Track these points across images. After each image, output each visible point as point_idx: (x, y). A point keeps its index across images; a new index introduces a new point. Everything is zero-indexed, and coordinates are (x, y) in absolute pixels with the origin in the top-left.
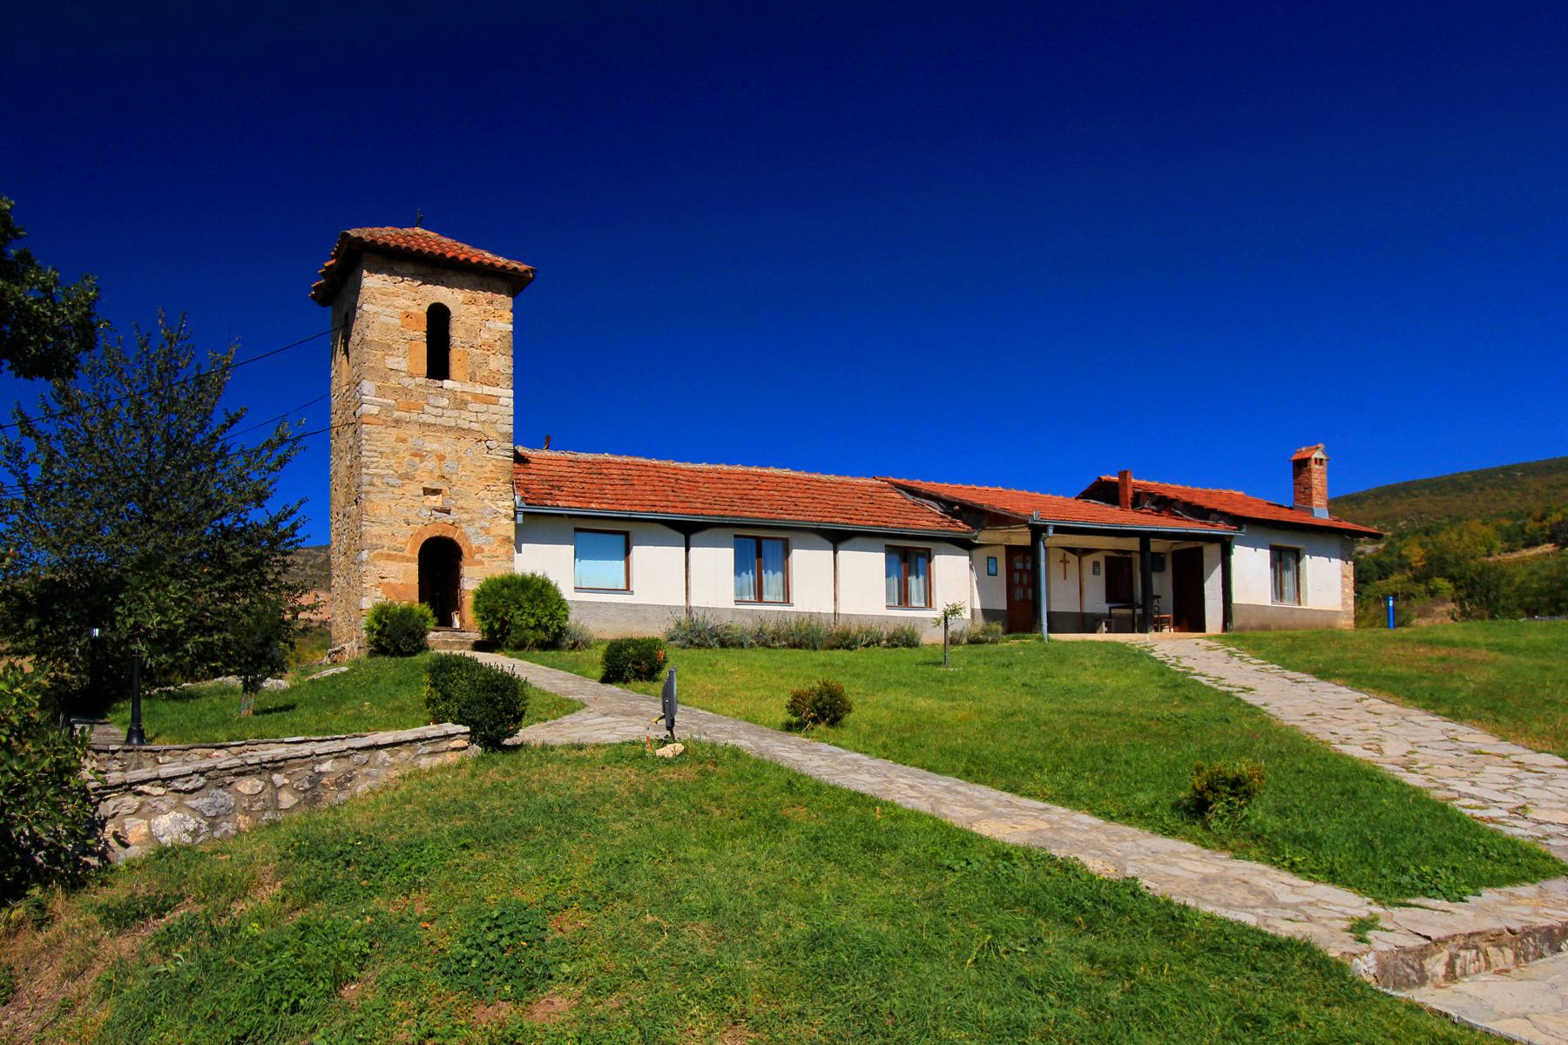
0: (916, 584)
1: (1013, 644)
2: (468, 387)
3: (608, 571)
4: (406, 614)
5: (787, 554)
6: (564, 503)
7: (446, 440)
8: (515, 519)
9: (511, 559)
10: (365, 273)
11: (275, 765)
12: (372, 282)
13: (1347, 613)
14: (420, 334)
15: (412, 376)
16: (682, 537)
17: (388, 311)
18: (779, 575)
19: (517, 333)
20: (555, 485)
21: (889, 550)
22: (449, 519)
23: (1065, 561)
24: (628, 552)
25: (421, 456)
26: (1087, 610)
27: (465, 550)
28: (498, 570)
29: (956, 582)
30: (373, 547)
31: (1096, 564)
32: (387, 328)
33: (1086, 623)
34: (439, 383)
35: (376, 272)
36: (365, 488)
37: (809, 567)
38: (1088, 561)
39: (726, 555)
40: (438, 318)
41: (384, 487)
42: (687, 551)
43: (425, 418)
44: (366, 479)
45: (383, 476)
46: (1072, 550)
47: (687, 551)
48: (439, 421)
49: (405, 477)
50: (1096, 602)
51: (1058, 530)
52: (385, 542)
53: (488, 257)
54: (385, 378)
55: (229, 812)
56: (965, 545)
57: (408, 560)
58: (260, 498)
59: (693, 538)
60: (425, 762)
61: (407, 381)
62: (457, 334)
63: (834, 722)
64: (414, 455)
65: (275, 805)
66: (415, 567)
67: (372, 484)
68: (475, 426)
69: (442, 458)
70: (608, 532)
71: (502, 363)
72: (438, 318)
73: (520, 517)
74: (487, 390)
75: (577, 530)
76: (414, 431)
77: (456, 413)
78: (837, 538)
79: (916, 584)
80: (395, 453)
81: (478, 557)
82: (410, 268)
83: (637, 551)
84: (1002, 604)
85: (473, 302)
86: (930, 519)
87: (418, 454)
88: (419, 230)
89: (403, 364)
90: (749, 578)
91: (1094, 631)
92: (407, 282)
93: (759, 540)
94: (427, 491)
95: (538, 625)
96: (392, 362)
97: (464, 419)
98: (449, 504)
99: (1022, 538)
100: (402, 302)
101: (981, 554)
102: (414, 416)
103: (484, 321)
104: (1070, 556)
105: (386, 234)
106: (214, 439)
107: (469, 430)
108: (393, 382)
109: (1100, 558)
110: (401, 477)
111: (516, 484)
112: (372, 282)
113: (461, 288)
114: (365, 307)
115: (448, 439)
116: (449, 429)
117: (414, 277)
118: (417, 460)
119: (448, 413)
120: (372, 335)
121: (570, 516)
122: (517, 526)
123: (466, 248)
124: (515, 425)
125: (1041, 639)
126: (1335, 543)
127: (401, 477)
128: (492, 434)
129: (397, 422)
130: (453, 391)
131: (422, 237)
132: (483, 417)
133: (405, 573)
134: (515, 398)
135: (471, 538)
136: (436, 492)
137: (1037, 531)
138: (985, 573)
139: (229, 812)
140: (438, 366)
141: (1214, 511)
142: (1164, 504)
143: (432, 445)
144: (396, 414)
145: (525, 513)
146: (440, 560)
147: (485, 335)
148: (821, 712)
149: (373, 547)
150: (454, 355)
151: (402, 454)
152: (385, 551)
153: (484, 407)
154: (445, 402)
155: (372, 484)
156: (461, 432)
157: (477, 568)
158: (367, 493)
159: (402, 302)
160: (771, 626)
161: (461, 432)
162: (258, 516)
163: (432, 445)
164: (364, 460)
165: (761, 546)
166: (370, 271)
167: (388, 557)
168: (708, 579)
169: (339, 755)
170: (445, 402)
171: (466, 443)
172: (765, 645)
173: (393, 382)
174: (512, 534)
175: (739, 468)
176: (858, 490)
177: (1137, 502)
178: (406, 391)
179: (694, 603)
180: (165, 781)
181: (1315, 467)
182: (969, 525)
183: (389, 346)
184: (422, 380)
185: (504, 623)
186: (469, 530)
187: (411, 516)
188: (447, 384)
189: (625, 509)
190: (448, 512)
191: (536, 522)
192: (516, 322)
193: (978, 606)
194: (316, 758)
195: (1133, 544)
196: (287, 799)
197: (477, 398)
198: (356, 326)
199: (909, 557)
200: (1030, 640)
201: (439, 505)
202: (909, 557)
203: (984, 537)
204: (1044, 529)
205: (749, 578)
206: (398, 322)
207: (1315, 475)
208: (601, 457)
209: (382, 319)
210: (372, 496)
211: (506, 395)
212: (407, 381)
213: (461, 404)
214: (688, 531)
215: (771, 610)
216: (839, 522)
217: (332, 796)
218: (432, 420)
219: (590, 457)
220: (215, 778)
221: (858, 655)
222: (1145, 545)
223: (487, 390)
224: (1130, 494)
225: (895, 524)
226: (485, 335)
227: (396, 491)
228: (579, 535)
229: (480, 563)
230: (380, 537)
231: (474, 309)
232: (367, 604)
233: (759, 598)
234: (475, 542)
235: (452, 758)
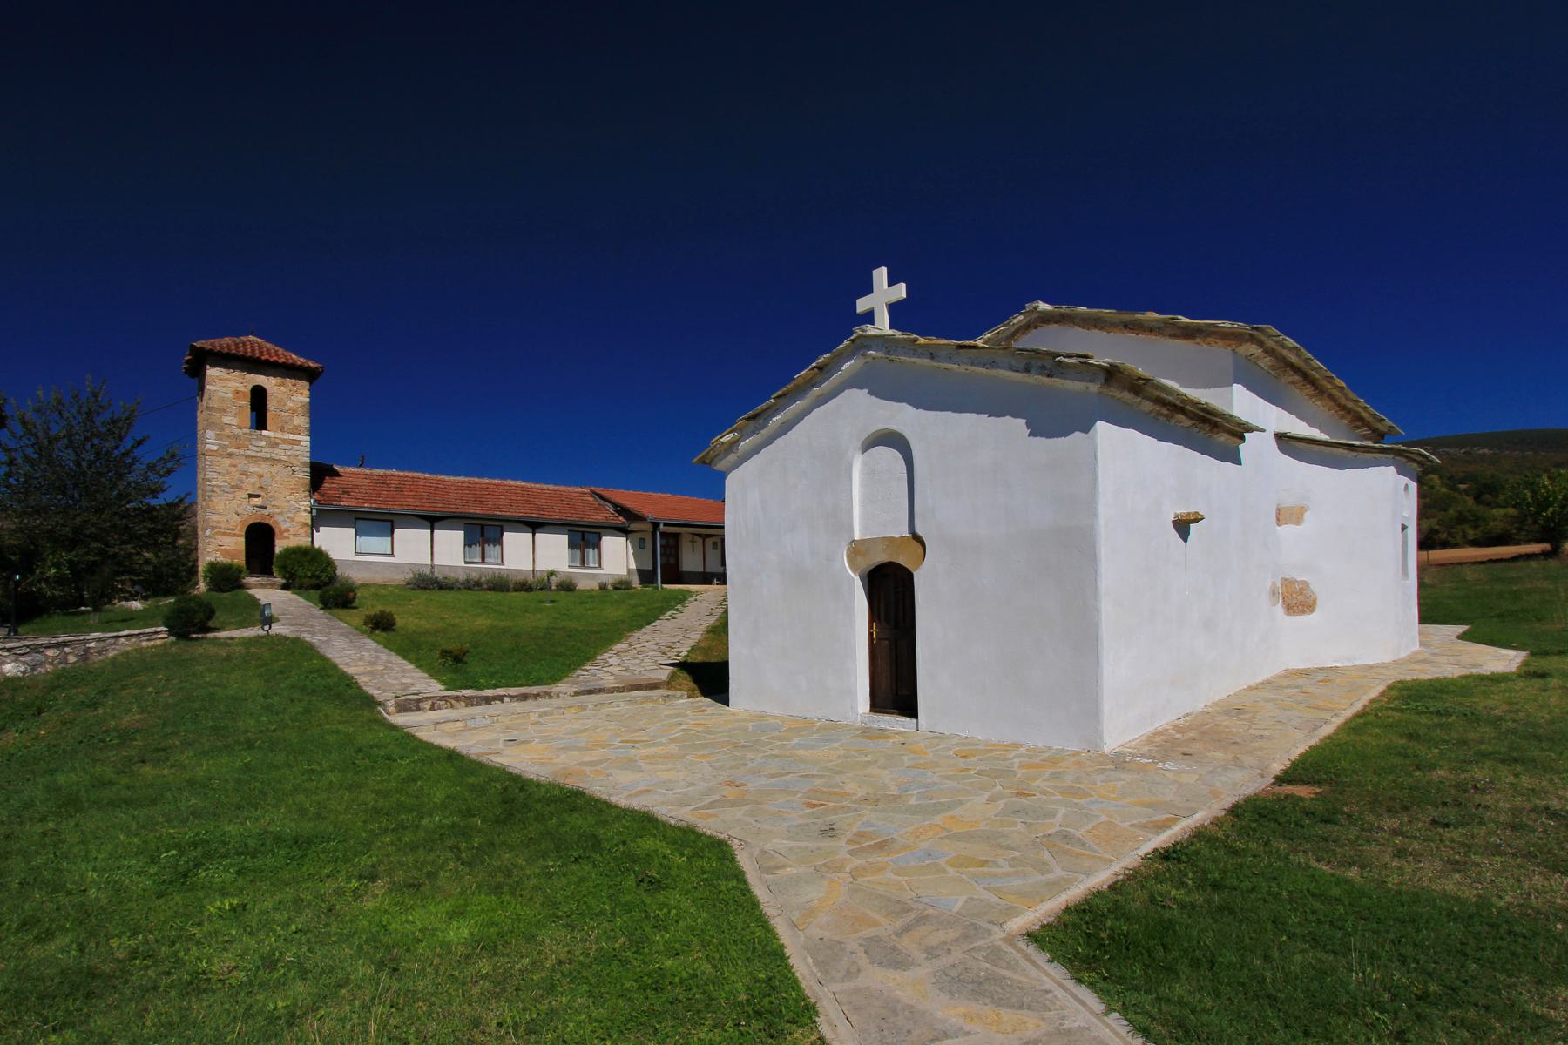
2: (279, 435)
3: (377, 543)
6: (345, 503)
11: (66, 644)
14: (246, 404)
19: (312, 404)
21: (570, 533)
28: (302, 541)
29: (618, 557)
30: (213, 528)
32: (223, 400)
38: (709, 541)
39: (460, 535)
40: (259, 398)
46: (699, 535)
49: (238, 487)
53: (294, 358)
55: (41, 664)
56: (622, 531)
58: (154, 493)
60: (144, 644)
63: (384, 630)
65: (65, 660)
69: (261, 476)
70: (383, 521)
71: (302, 421)
72: (259, 398)
74: (291, 436)
78: (534, 526)
79: (591, 553)
85: (283, 384)
86: (608, 514)
87: (245, 473)
88: (251, 338)
89: (235, 421)
90: (478, 549)
91: (710, 583)
92: (237, 373)
93: (483, 527)
94: (251, 496)
95: (313, 576)
96: (226, 420)
101: (636, 536)
103: (290, 398)
105: (224, 343)
106: (126, 454)
108: (227, 431)
112: (212, 372)
116: (266, 459)
123: (281, 351)
128: (295, 462)
129: (230, 455)
131: (253, 343)
135: (281, 523)
136: (257, 496)
137: (656, 525)
138: (640, 546)
139: (41, 664)
140: (260, 422)
143: (254, 469)
146: (260, 536)
147: (290, 404)
148: (381, 625)
149: (213, 528)
150: (269, 415)
156: (274, 461)
160: (474, 575)
161: (274, 461)
162: (154, 502)
163: (254, 469)
165: (484, 531)
166: (213, 366)
167: (224, 534)
168: (448, 550)
169: (99, 640)
171: (279, 467)
172: (469, 589)
173: (227, 431)
175: (486, 480)
176: (573, 496)
178: (236, 437)
180: (9, 650)
182: (626, 522)
186: (277, 517)
188: (264, 433)
191: (323, 516)
193: (633, 566)
194: (88, 641)
196: (72, 659)
197: (285, 441)
199: (584, 538)
202: (584, 538)
203: (634, 526)
208: (389, 472)
211: (305, 440)
214: (433, 521)
217: (96, 658)
219: (381, 472)
220: (35, 649)
223: (291, 436)
225: (574, 518)
226: (290, 404)
233: (483, 561)
235: (159, 642)
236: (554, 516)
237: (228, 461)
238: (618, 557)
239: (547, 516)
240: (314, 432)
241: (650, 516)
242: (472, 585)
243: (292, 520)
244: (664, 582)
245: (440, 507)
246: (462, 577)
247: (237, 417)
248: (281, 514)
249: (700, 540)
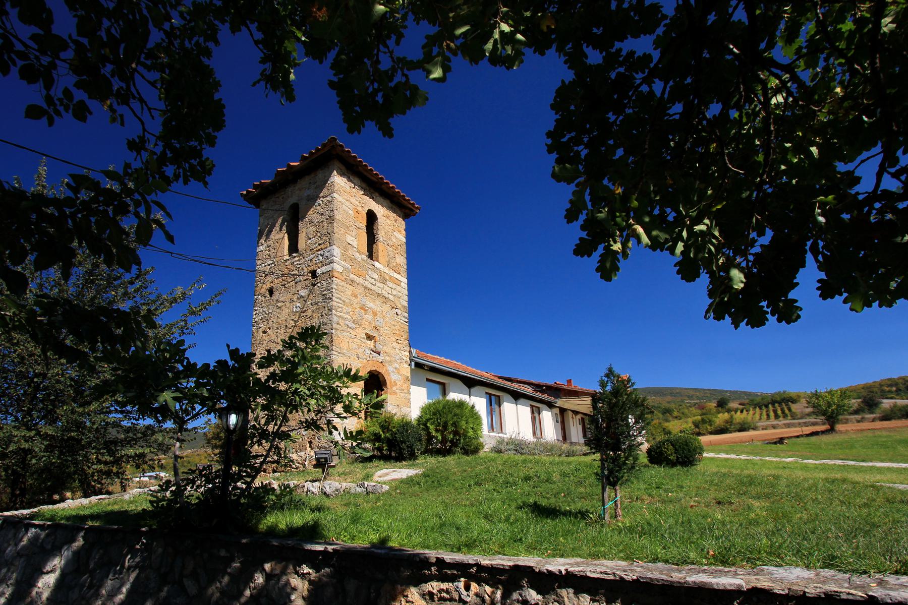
25: (365, 310)
27: (388, 382)
43: (367, 284)
44: (335, 319)
45: (345, 319)
48: (374, 288)
61: (357, 255)
67: (338, 324)
68: (391, 297)
69: (375, 314)
71: (401, 260)
76: (360, 290)
77: (381, 285)
87: (363, 308)
96: (350, 239)
98: (379, 348)
102: (361, 280)
110: (354, 322)
115: (378, 302)
116: (379, 295)
117: (362, 188)
121: (433, 370)
132: (394, 293)
144: (352, 276)
153: (394, 286)
157: (394, 397)
170: (376, 276)
171: (386, 308)
184: (366, 258)
212: (357, 255)
218: (370, 286)
227: (352, 331)
247: (358, 240)
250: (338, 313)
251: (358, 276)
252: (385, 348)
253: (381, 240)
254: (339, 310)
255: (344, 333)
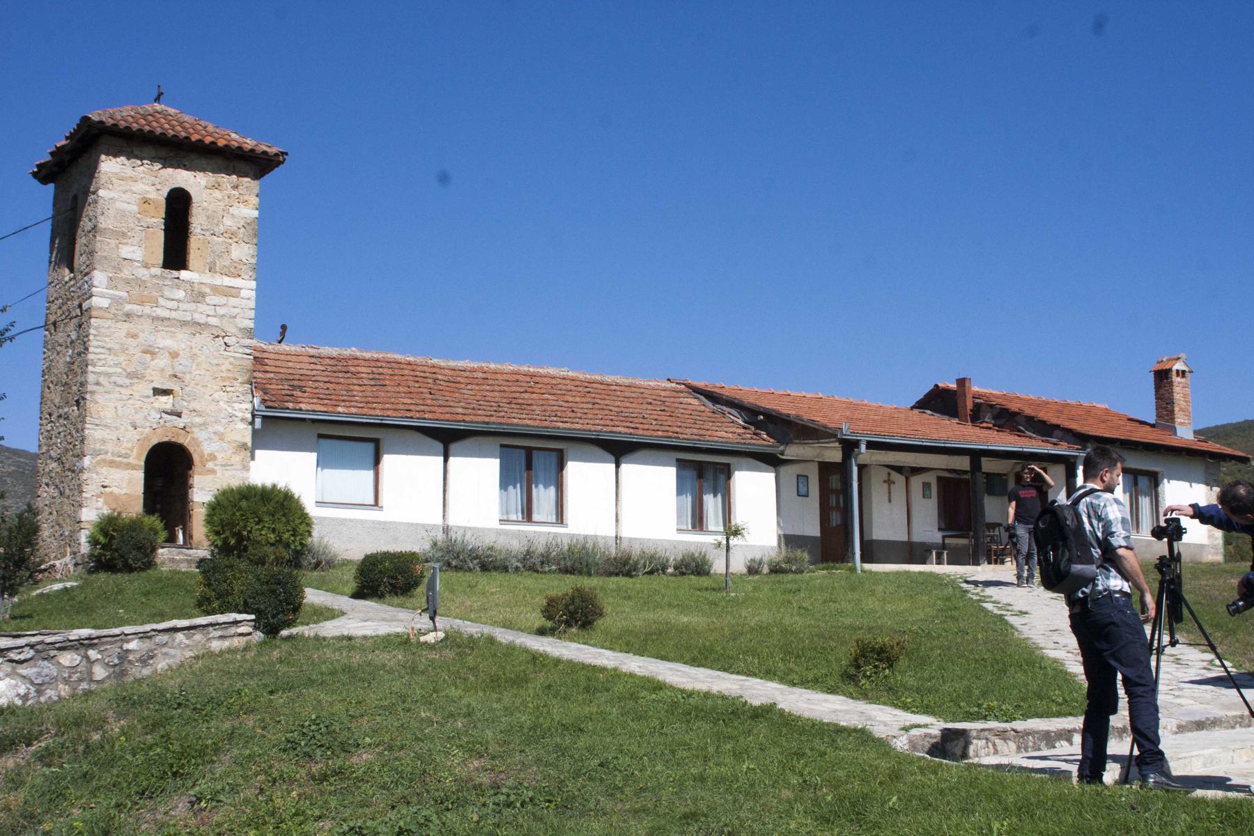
0: (712, 503)
1: (820, 575)
2: (207, 278)
4: (134, 525)
5: (561, 467)
6: (308, 407)
7: (180, 336)
8: (252, 423)
9: (246, 468)
10: (103, 157)
12: (110, 166)
13: (1215, 547)
14: (157, 221)
15: (146, 266)
16: (440, 446)
17: (125, 197)
18: (552, 491)
20: (297, 385)
21: (681, 465)
22: (180, 423)
23: (889, 482)
24: (377, 461)
25: (153, 354)
26: (916, 538)
27: (196, 458)
29: (758, 505)
30: (96, 453)
31: (926, 486)
32: (123, 214)
33: (914, 552)
34: (175, 273)
35: (115, 156)
36: (90, 388)
37: (586, 478)
38: (917, 482)
40: (178, 204)
41: (111, 387)
42: (446, 461)
44: (91, 378)
45: (109, 375)
46: (899, 469)
47: (446, 461)
48: (174, 315)
49: (133, 375)
50: (927, 529)
51: (871, 445)
52: (110, 447)
54: (118, 269)
56: (770, 460)
57: (134, 467)
59: (453, 447)
62: (198, 221)
64: (145, 352)
66: (140, 475)
67: (98, 384)
68: (213, 321)
69: (174, 355)
70: (358, 438)
71: (244, 252)
72: (178, 207)
73: (258, 421)
74: (228, 281)
75: (321, 436)
76: (147, 325)
77: (192, 306)
79: (712, 503)
80: (124, 349)
81: (210, 465)
82: (150, 150)
83: (388, 460)
84: (814, 530)
85: (217, 186)
86: (730, 431)
87: (150, 351)
93: (529, 452)
94: (158, 392)
96: (125, 251)
97: (201, 313)
98: (181, 405)
99: (834, 454)
100: (140, 187)
101: (789, 472)
102: (147, 310)
104: (895, 476)
107: (206, 325)
108: (126, 273)
109: (931, 478)
110: (131, 375)
111: (255, 385)
113: (203, 170)
114: (101, 193)
116: (184, 323)
117: (153, 159)
118: (148, 357)
119: (183, 306)
120: (104, 223)
121: (314, 421)
122: (255, 432)
124: (257, 319)
125: (853, 570)
126: (1198, 467)
127: (131, 375)
128: (231, 329)
129: (128, 315)
130: (191, 283)
132: (221, 311)
133: (130, 482)
134: (258, 290)
137: (849, 447)
141: (1057, 427)
142: (1006, 418)
143: (165, 341)
144: (128, 307)
145: (264, 417)
146: (168, 467)
147: (228, 222)
150: (194, 244)
151: (132, 351)
152: (109, 457)
153: (223, 300)
154: (181, 294)
155: (98, 384)
156: (197, 327)
157: (209, 477)
158: (92, 393)
159: (140, 187)
161: (197, 327)
164: (90, 356)
165: (533, 457)
166: (107, 154)
171: (203, 339)
173: (126, 273)
174: (248, 440)
177: (976, 416)
178: (140, 283)
179: (452, 521)
181: (1177, 380)
183: (124, 234)
184: (158, 271)
185: (240, 538)
186: (201, 435)
187: (139, 419)
188: (184, 274)
189: (376, 413)
190: (179, 415)
191: (275, 427)
192: (259, 208)
195: (963, 463)
197: (216, 290)
198: (88, 211)
199: (705, 471)
200: (840, 572)
201: (169, 407)
203: (792, 451)
204: (856, 444)
205: (515, 493)
206: (135, 208)
207: (1177, 389)
209: (119, 205)
210: (97, 397)
211: (248, 287)
212: (143, 273)
213: (198, 296)
215: (542, 532)
216: (621, 431)
218: (166, 314)
221: (639, 583)
222: (976, 466)
223: (228, 281)
224: (970, 405)
225: (688, 435)
226: (228, 222)
227: (123, 391)
228: (323, 441)
229: (213, 472)
230: (104, 442)
231: (217, 194)
232: (90, 514)
234: (207, 448)
236: (657, 436)
237: (125, 327)
238: (758, 505)
239: (641, 435)
240: (263, 271)
241: (846, 430)
242: (533, 563)
243: (221, 437)
244: (865, 559)
245: (456, 414)
246: (517, 546)
248: (204, 425)
249: (899, 479)
250: (97, 369)
251: (142, 303)
252: (194, 405)
253: (198, 230)
254: (100, 363)
255: (107, 396)
